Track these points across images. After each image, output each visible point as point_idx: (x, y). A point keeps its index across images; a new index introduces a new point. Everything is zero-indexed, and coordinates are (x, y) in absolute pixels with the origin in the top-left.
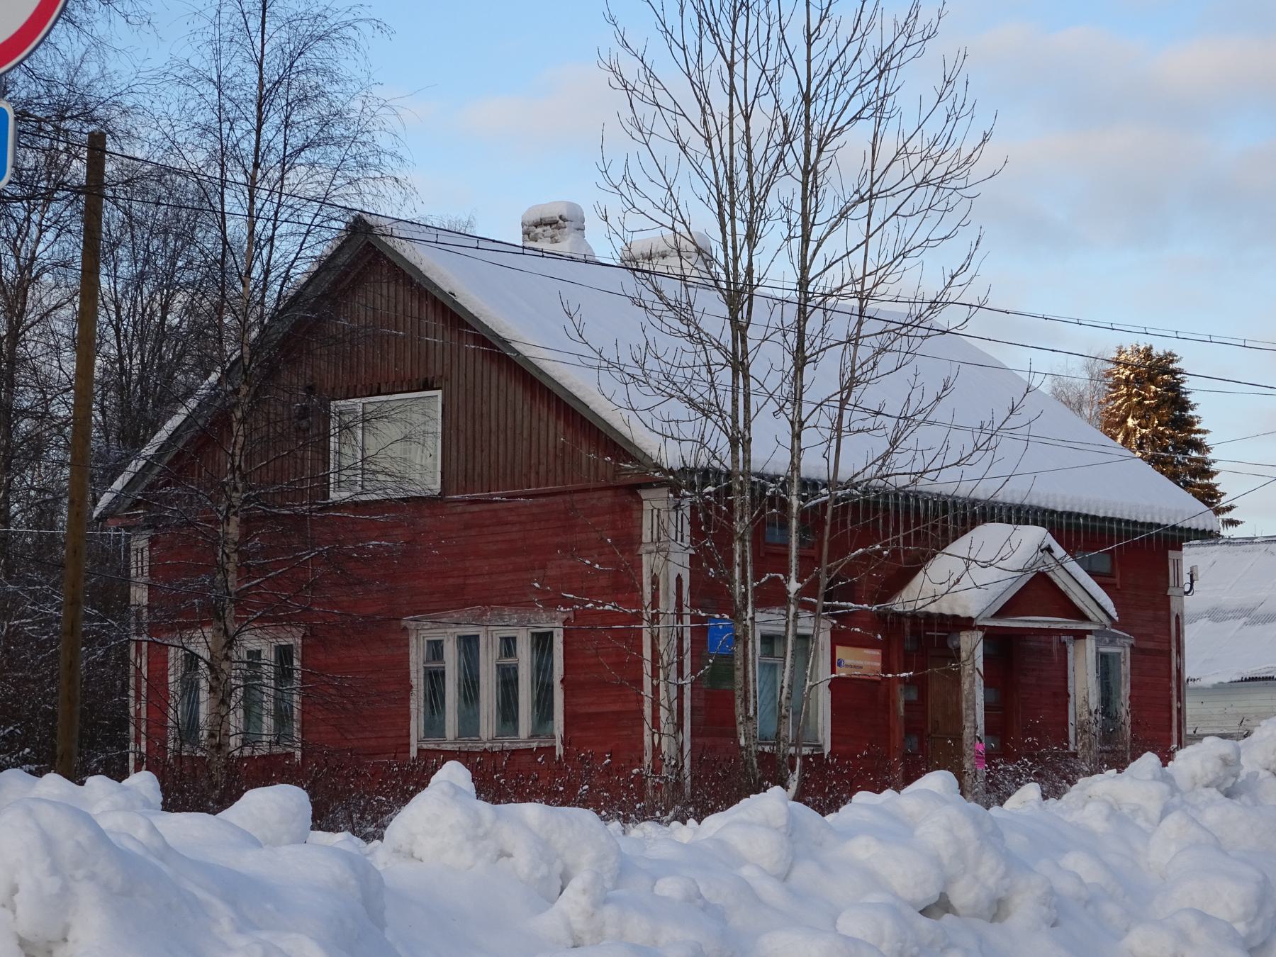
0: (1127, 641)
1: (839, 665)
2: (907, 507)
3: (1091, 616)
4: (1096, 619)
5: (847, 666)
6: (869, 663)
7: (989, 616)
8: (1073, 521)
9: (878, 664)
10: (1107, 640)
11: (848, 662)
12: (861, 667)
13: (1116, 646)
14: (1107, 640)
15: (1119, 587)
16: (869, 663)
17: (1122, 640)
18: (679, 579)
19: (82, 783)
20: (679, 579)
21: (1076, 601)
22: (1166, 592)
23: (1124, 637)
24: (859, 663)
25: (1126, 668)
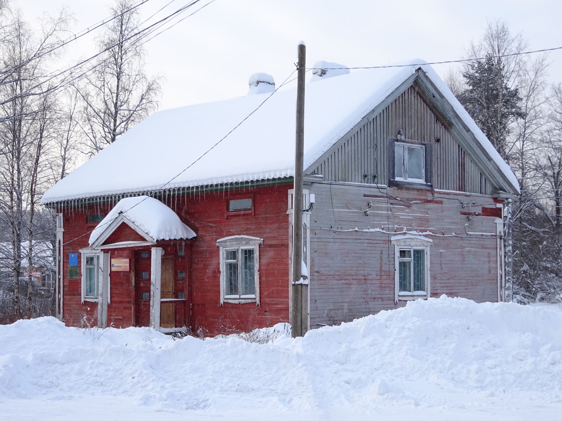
0: (257, 242)
1: (113, 267)
2: (169, 195)
3: (147, 239)
4: (149, 240)
5: (115, 266)
6: (124, 265)
7: (100, 245)
8: (190, 191)
9: (128, 265)
10: (244, 242)
11: (116, 265)
12: (121, 267)
13: (250, 245)
14: (244, 242)
15: (253, 215)
16: (124, 265)
17: (253, 242)
18: (60, 241)
19: (448, 297)
20: (60, 241)
21: (139, 233)
22: (286, 212)
23: (255, 240)
24: (120, 265)
25: (256, 255)
